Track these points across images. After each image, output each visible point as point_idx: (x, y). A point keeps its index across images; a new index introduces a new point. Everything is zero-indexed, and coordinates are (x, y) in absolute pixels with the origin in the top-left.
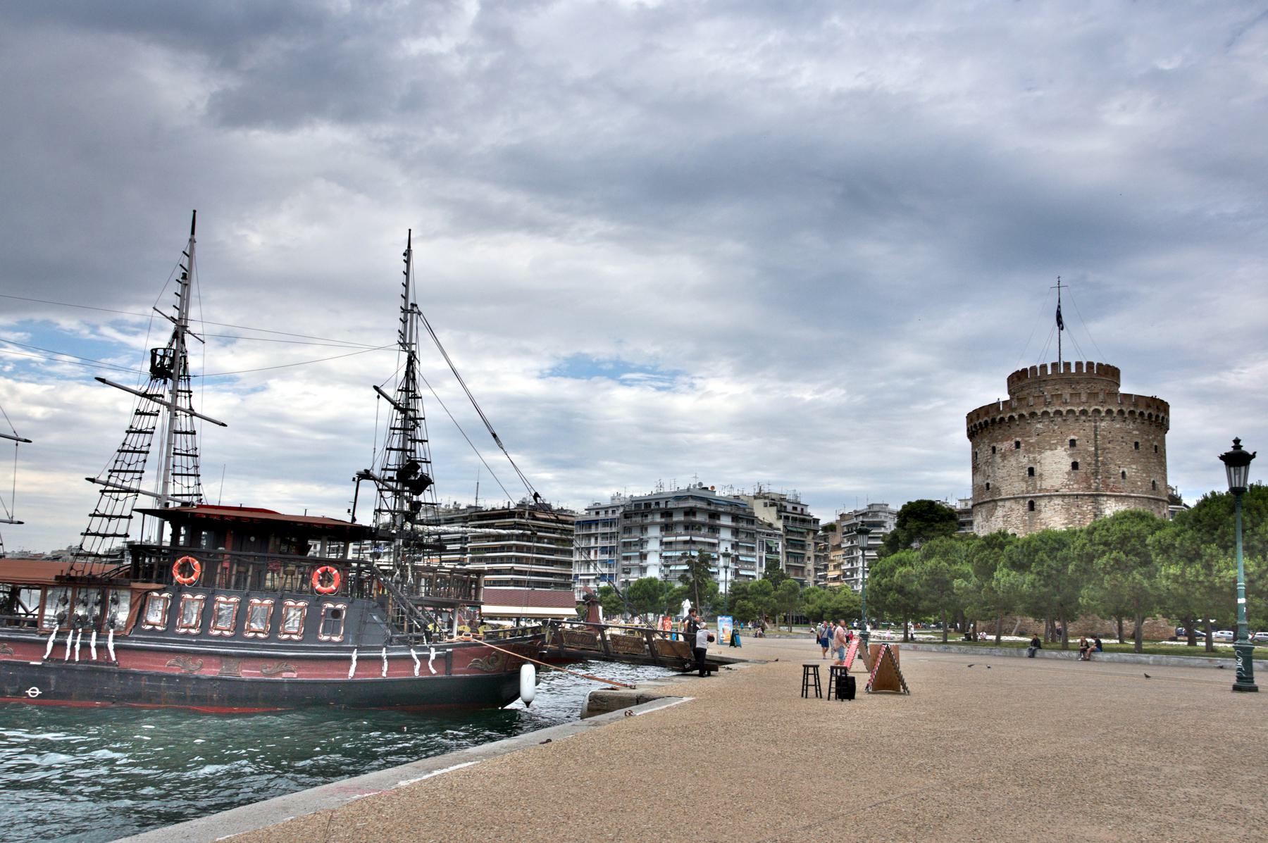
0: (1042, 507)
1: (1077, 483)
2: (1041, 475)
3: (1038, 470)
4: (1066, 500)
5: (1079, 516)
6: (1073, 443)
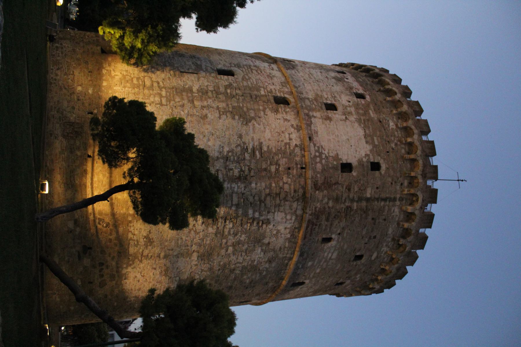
1: (324, 170)
2: (329, 119)
3: (336, 116)
4: (297, 150)
5: (273, 168)
6: (375, 166)
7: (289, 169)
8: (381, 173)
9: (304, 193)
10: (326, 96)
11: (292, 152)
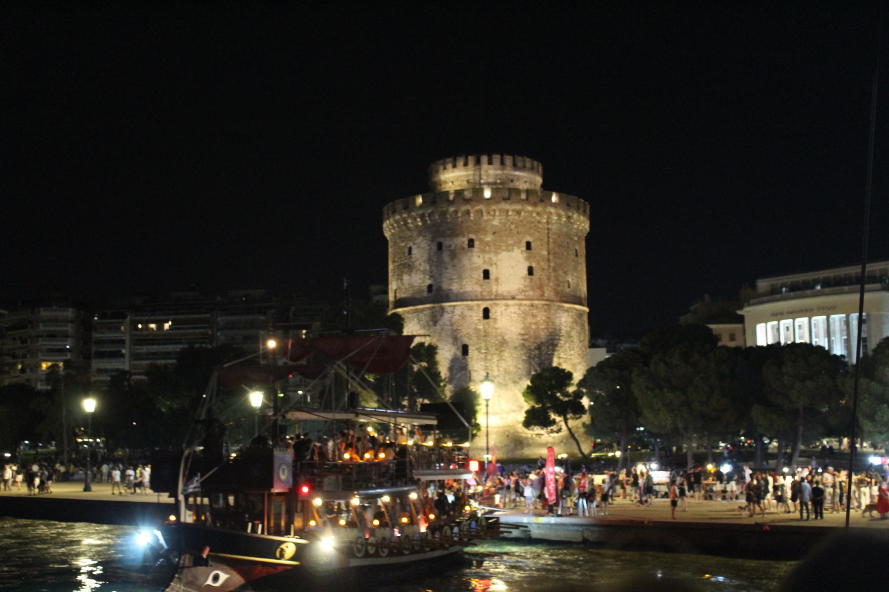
0: (499, 313)
1: (533, 290)
2: (497, 280)
4: (523, 308)
6: (528, 246)
7: (533, 315)
8: (533, 242)
9: (547, 305)
10: (477, 276)
11: (524, 313)
